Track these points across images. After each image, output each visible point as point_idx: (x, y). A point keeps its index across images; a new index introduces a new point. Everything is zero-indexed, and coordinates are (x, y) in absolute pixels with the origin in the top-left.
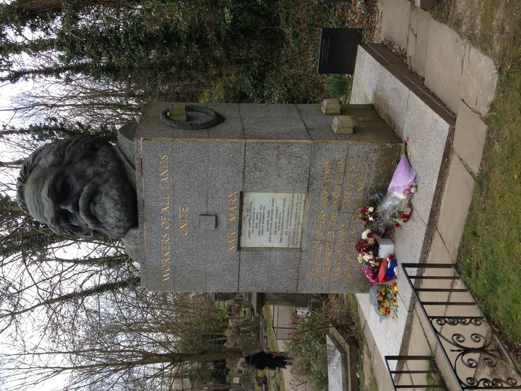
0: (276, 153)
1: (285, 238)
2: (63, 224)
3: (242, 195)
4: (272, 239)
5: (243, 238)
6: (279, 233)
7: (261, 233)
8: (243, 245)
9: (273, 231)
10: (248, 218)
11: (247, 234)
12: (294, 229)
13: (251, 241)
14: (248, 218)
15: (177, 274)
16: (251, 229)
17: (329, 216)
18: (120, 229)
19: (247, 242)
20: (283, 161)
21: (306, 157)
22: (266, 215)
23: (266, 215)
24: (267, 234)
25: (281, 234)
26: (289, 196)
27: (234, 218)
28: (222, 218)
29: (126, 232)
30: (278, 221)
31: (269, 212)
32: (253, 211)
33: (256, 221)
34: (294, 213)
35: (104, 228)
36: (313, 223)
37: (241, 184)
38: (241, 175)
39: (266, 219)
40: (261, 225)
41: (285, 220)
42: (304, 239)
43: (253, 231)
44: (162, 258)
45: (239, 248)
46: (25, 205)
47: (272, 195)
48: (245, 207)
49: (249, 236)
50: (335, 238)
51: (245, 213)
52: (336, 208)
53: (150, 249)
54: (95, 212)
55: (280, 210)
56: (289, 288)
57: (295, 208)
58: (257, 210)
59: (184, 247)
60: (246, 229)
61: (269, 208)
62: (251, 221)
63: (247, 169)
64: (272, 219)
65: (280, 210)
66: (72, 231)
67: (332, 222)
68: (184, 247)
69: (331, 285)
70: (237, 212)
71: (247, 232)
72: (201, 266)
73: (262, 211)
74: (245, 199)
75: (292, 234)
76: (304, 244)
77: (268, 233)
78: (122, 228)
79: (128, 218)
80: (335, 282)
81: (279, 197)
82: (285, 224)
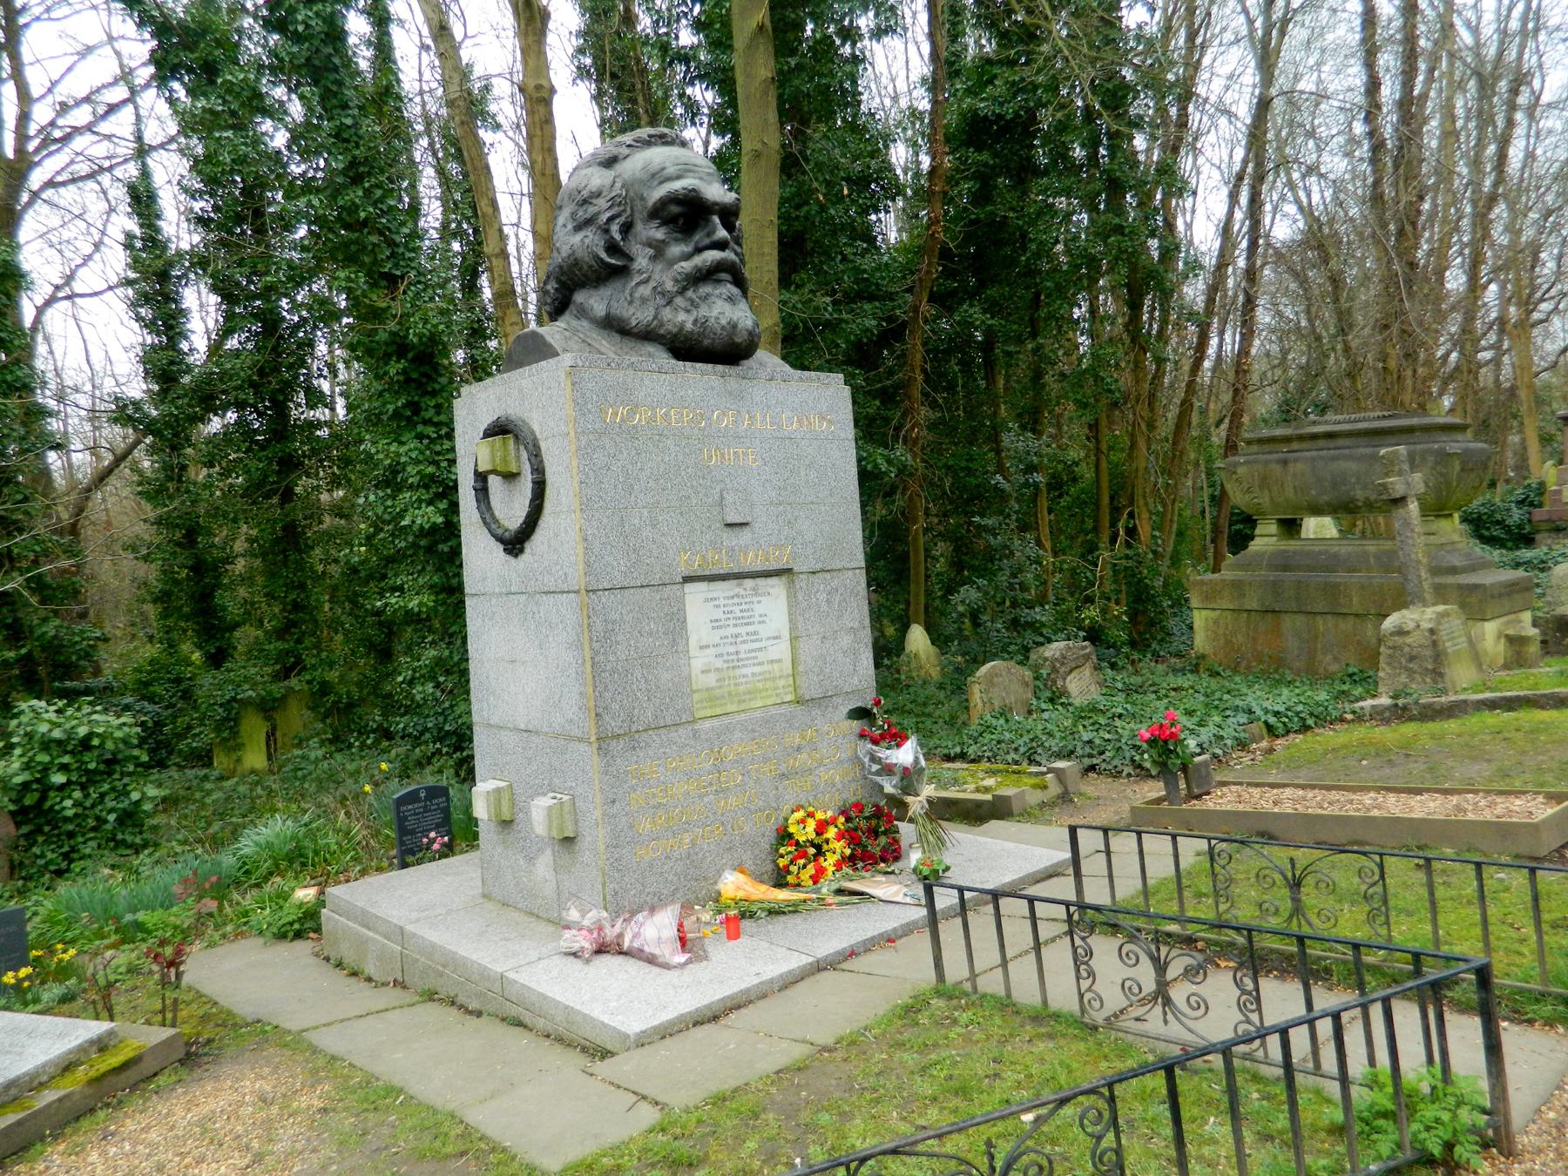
0: (856, 625)
1: (711, 680)
2: (675, 209)
3: (777, 573)
4: (708, 651)
5: (703, 586)
6: (719, 664)
7: (716, 624)
8: (689, 587)
9: (720, 650)
10: (742, 592)
11: (711, 595)
12: (730, 693)
13: (699, 604)
14: (742, 592)
15: (618, 440)
16: (722, 602)
17: (766, 760)
18: (696, 321)
19: (695, 594)
20: (846, 640)
21: (856, 682)
22: (750, 629)
23: (750, 629)
24: (715, 637)
25: (717, 670)
26: (788, 664)
27: (752, 562)
28: (745, 536)
29: (647, 335)
30: (742, 656)
31: (755, 633)
32: (755, 599)
33: (737, 609)
34: (760, 685)
35: (682, 292)
36: (753, 731)
37: (804, 569)
38: (819, 567)
39: (743, 630)
40: (732, 622)
41: (744, 671)
42: (715, 722)
43: (718, 606)
44: (653, 409)
45: (688, 579)
46: (666, 143)
47: (786, 634)
48: (761, 582)
49: (707, 600)
50: (728, 789)
51: (749, 583)
52: (783, 768)
53: (671, 384)
54: (719, 281)
55: (761, 656)
56: (607, 718)
57: (769, 684)
58: (759, 609)
59: (681, 458)
60: (722, 589)
61: (764, 631)
62: (736, 600)
63: (828, 576)
64: (744, 642)
65: (761, 656)
66: (622, 219)
67: (757, 771)
68: (681, 458)
69: (624, 819)
70: (759, 566)
71: (715, 595)
72: (641, 496)
73: (757, 619)
74: (774, 581)
75: (718, 692)
76: (707, 724)
77: (717, 640)
78: (696, 330)
79: (737, 345)
80: (631, 827)
81: (782, 650)
82: (738, 672)
